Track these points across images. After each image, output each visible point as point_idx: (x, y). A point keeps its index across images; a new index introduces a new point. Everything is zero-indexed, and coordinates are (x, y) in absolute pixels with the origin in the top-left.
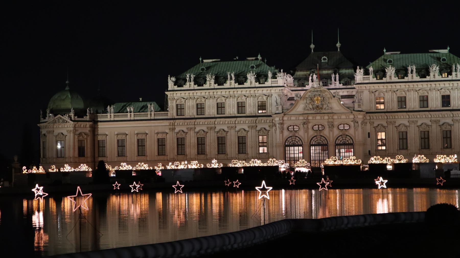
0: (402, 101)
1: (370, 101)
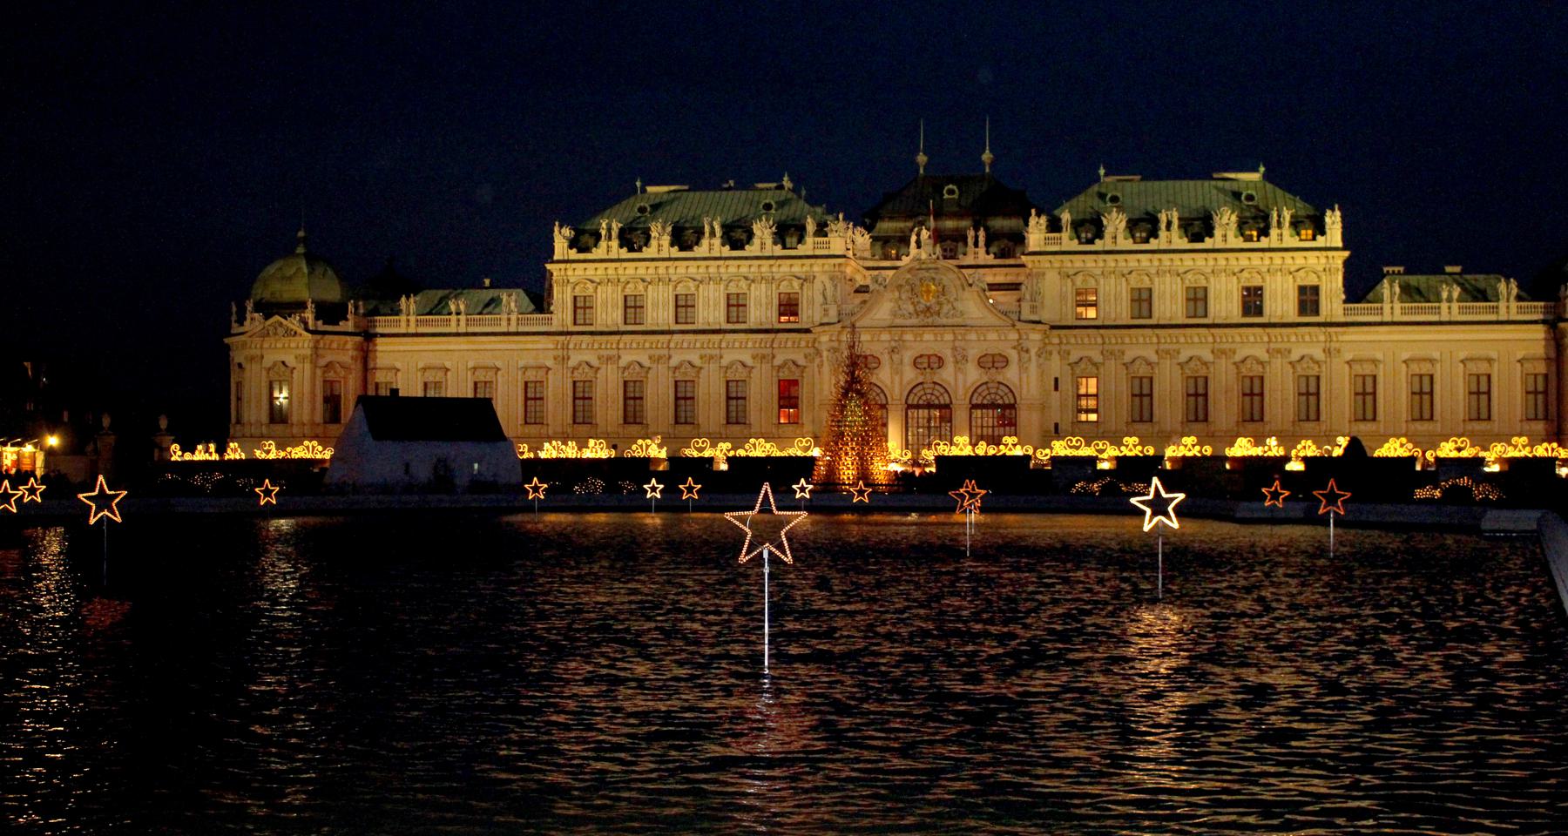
0: (1143, 300)
1: (1063, 297)
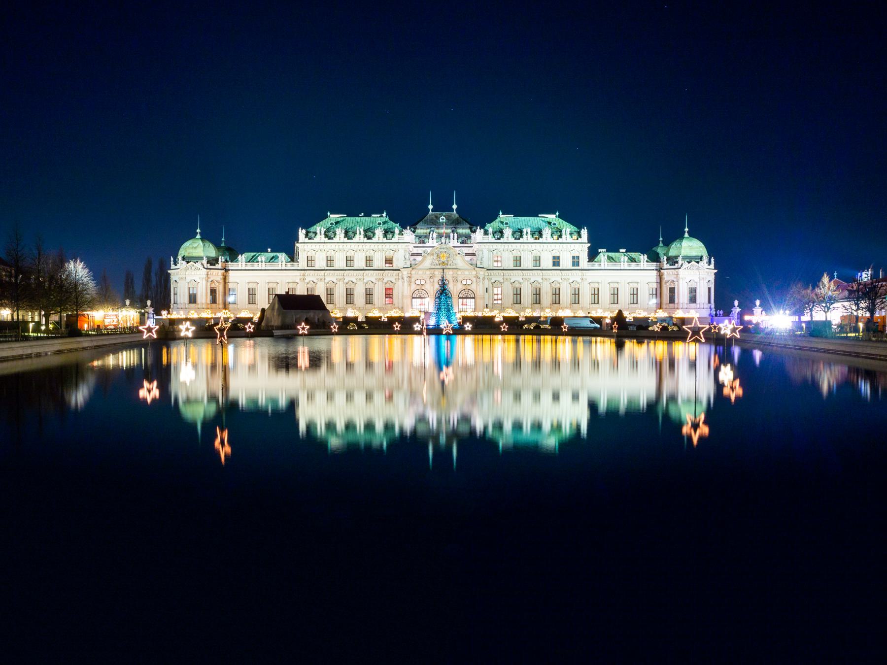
0: (518, 260)
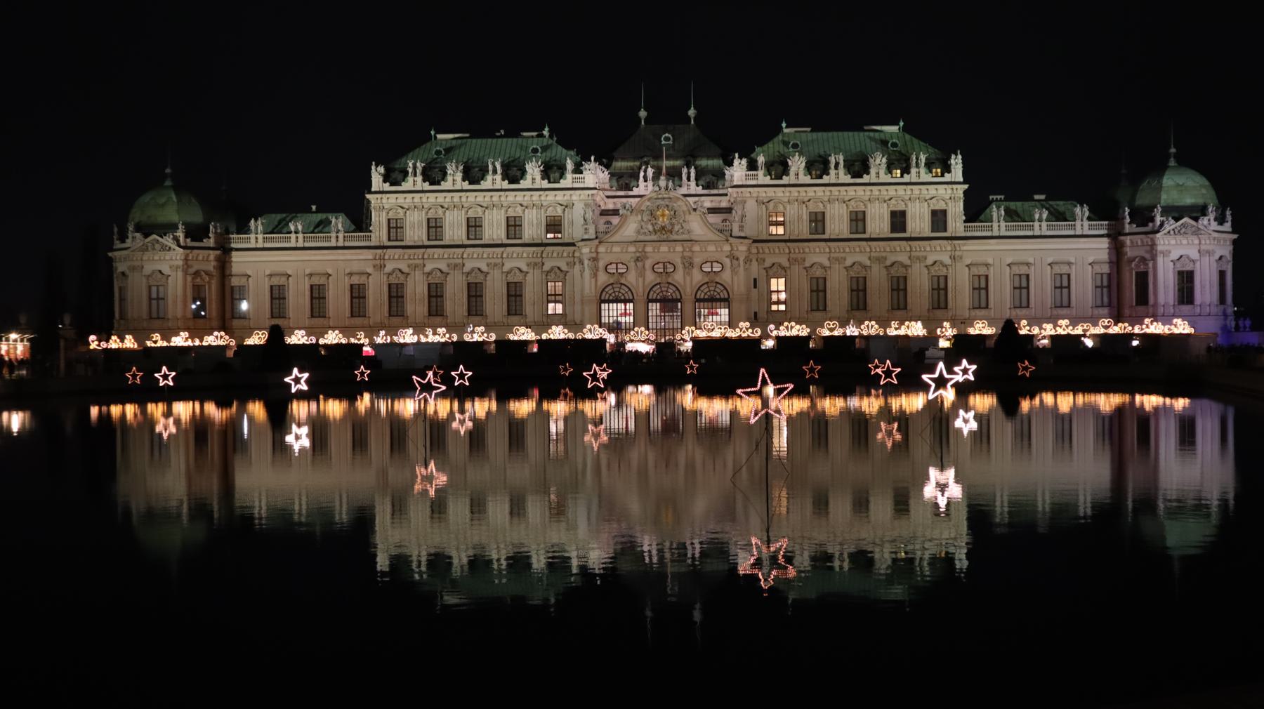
0: (818, 220)
1: (759, 219)
